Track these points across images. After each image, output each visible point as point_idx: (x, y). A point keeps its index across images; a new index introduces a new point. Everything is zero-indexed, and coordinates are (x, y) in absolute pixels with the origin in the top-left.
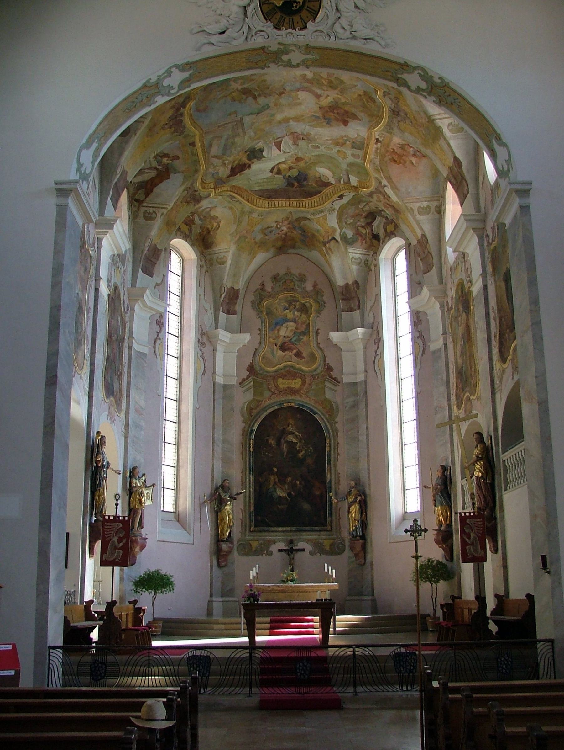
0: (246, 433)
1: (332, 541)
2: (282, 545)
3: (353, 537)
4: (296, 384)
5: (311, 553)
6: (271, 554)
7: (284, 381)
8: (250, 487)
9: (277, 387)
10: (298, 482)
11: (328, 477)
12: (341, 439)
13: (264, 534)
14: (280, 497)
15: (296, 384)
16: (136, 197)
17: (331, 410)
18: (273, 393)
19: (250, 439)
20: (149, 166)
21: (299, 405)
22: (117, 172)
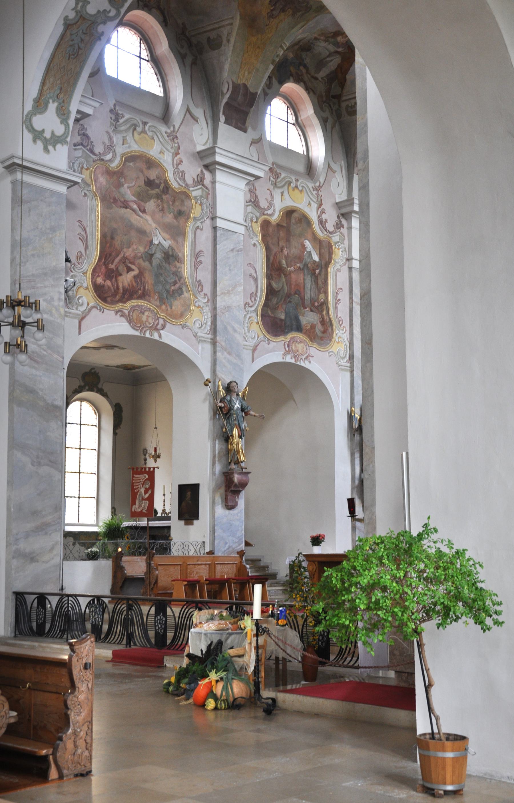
16: (332, 93)
20: (328, 53)
22: (222, 93)
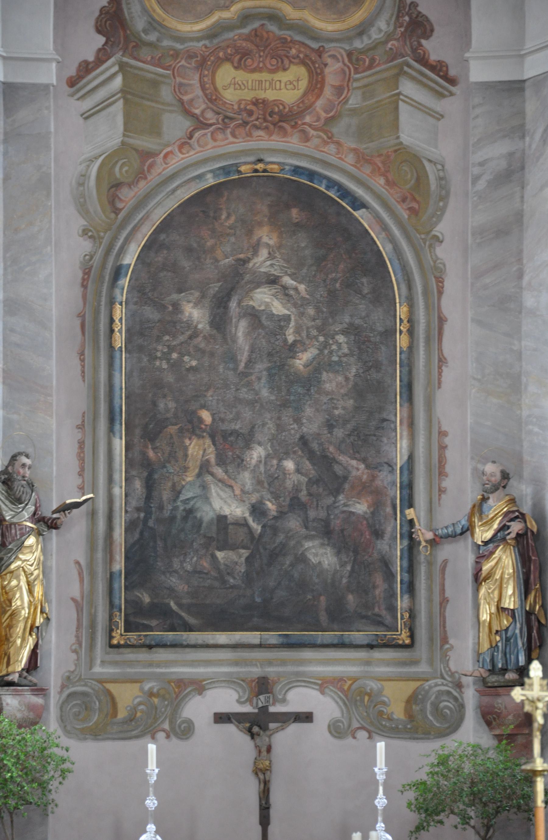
0: (98, 277)
1: (414, 685)
2: (228, 700)
3: (492, 671)
4: (286, 86)
5: (337, 730)
6: (185, 731)
7: (241, 76)
8: (110, 480)
9: (213, 98)
10: (289, 465)
11: (402, 447)
12: (455, 302)
13: (162, 655)
14: (222, 519)
15: (286, 86)
17: (418, 189)
18: (201, 124)
19: (111, 302)
21: (297, 170)
